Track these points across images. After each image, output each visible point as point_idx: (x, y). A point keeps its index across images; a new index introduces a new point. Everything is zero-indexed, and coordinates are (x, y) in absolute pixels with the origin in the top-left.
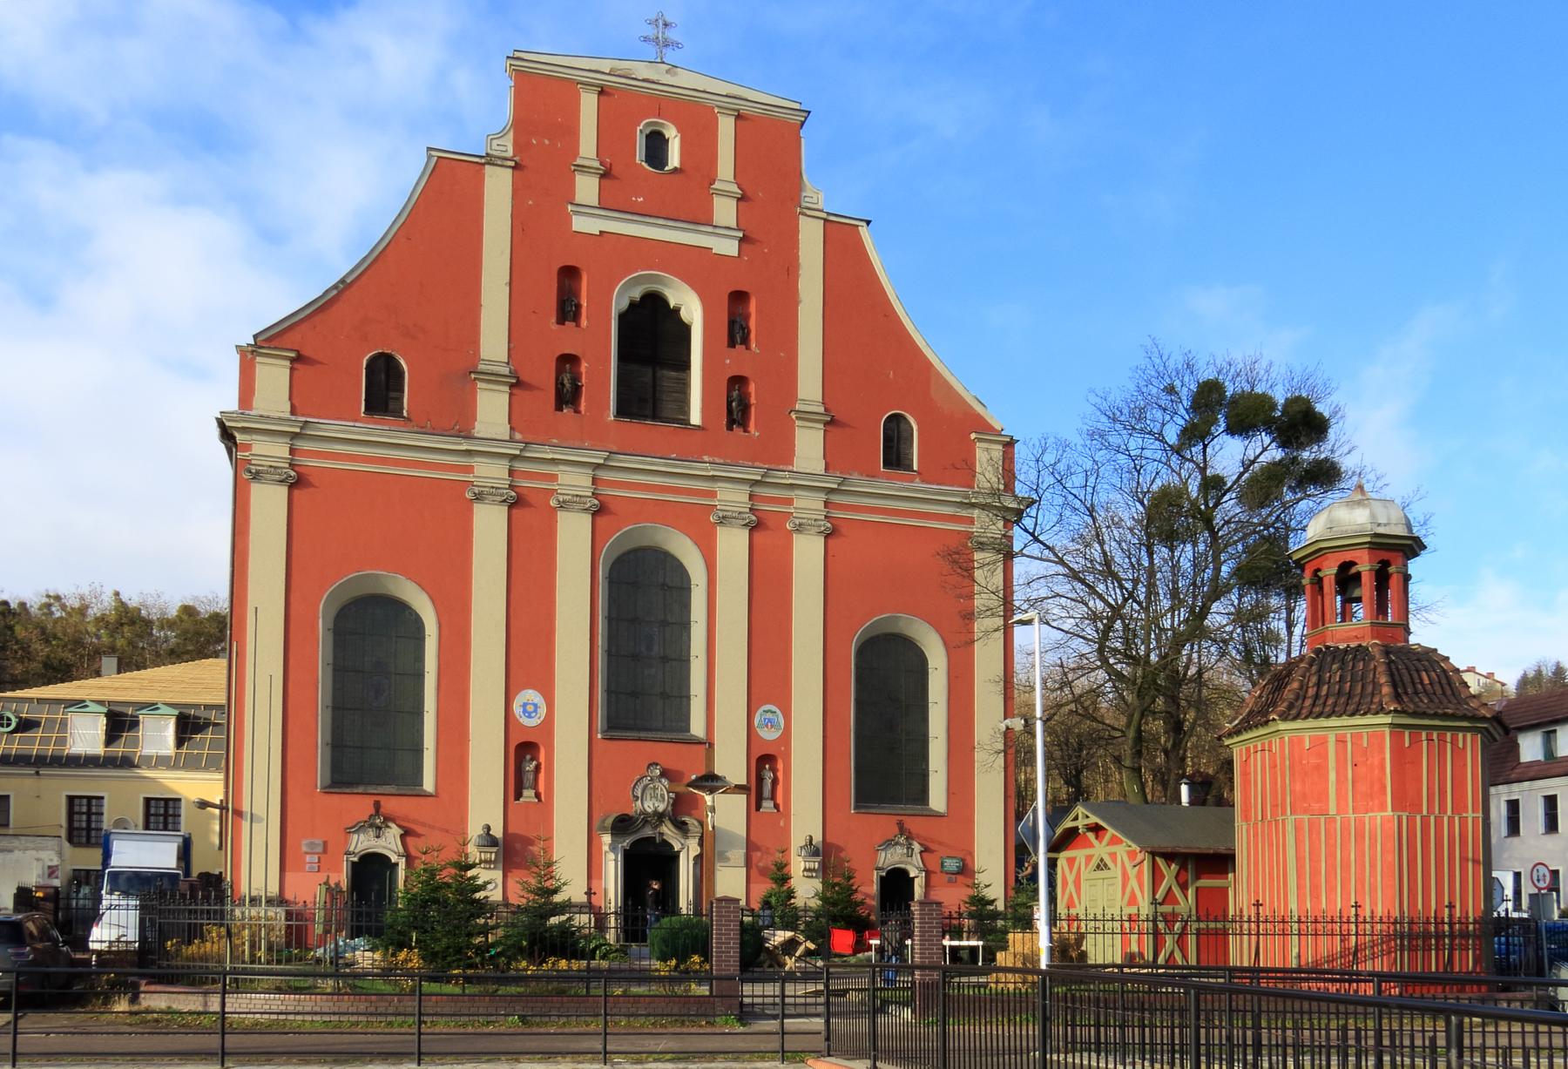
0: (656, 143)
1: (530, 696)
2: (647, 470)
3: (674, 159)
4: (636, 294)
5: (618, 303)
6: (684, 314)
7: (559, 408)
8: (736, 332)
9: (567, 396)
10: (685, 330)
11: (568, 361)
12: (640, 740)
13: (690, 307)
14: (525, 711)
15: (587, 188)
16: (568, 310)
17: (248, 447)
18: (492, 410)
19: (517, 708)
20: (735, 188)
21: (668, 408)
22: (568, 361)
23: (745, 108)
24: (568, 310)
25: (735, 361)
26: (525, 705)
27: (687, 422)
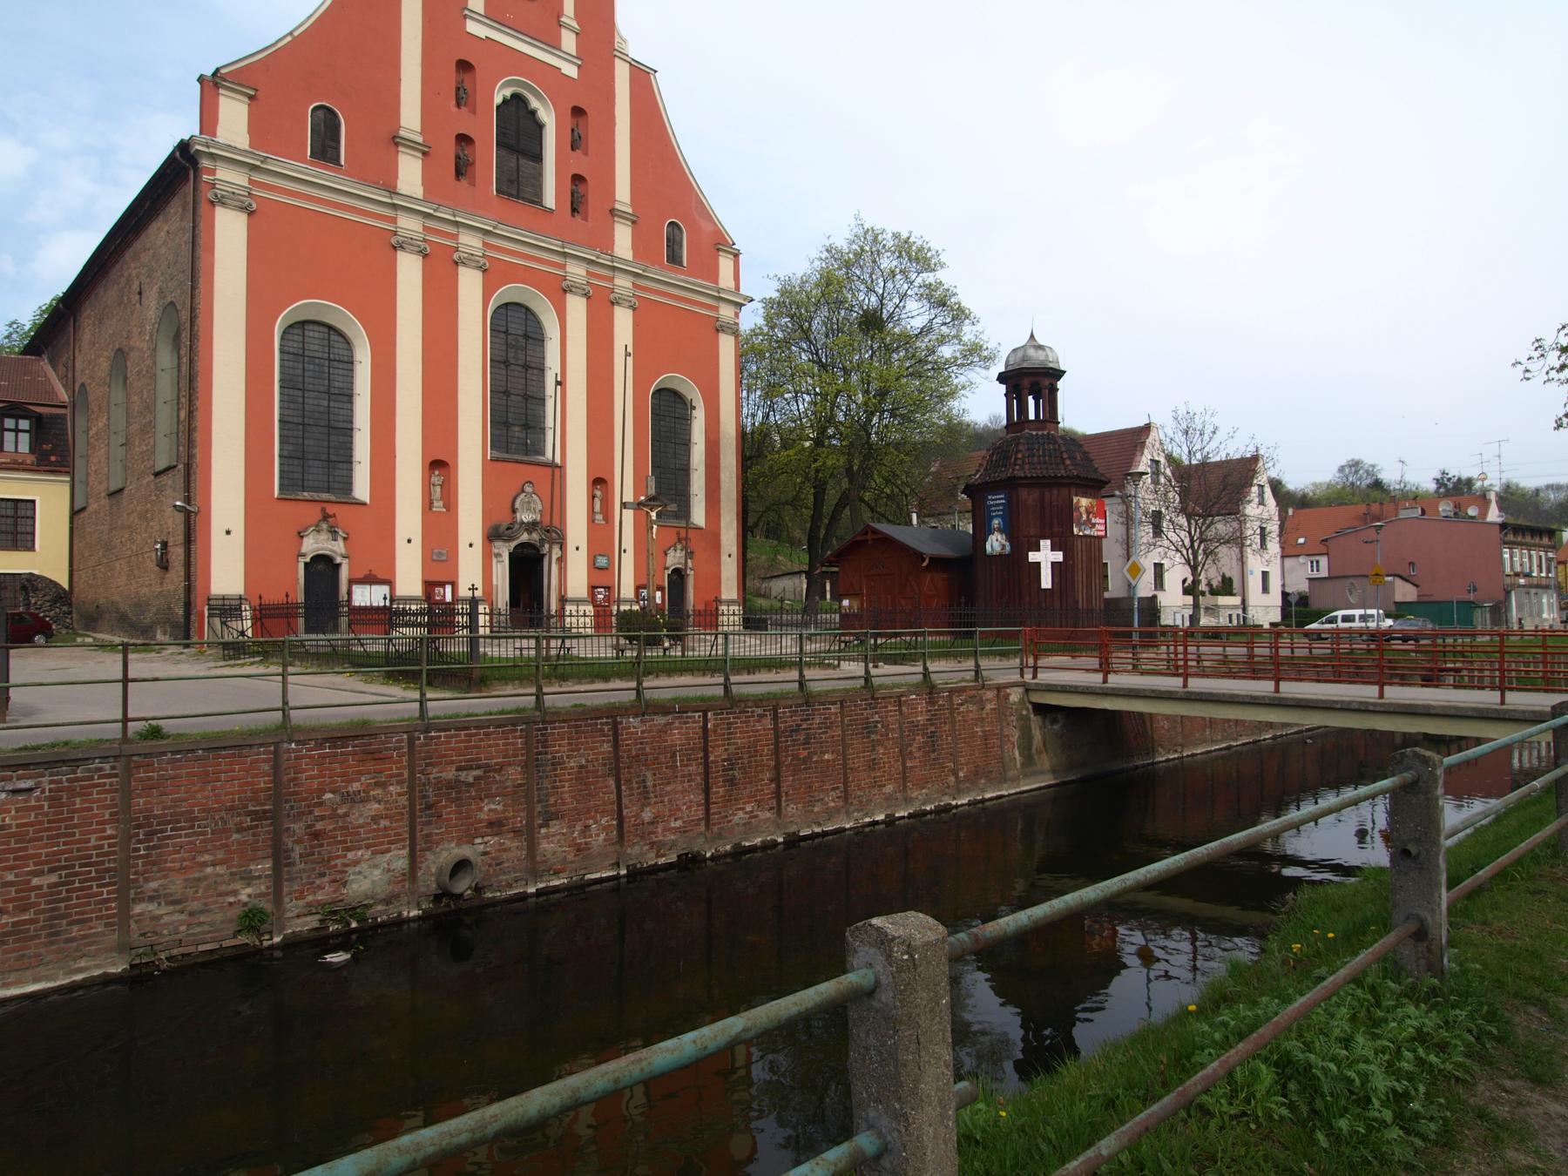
2: (521, 240)
4: (508, 92)
5: (498, 100)
8: (576, 142)
13: (547, 116)
22: (463, 140)
25: (579, 164)
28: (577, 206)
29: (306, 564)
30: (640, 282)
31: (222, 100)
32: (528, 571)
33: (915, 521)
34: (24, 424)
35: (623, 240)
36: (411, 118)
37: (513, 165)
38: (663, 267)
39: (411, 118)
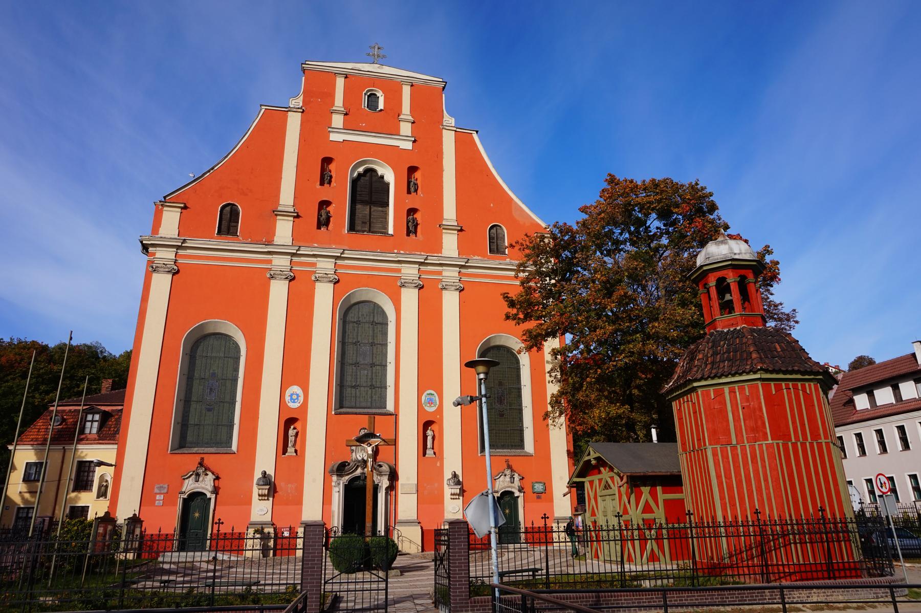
0: (373, 98)
1: (296, 389)
2: (364, 259)
3: (381, 106)
6: (386, 178)
7: (319, 228)
8: (411, 187)
9: (323, 222)
10: (387, 185)
11: (324, 204)
12: (356, 414)
13: (389, 175)
14: (291, 399)
15: (338, 121)
16: (325, 178)
17: (154, 254)
18: (284, 230)
19: (287, 398)
20: (410, 118)
21: (377, 226)
23: (414, 81)
24: (325, 178)
25: (411, 201)
26: (291, 395)
27: (386, 233)
28: (412, 229)
29: (184, 499)
30: (463, 271)
31: (444, 236)
32: (358, 499)
33: (655, 438)
34: (97, 417)
35: (450, 244)
36: (287, 197)
37: (367, 212)
38: (489, 258)
39: (287, 197)
